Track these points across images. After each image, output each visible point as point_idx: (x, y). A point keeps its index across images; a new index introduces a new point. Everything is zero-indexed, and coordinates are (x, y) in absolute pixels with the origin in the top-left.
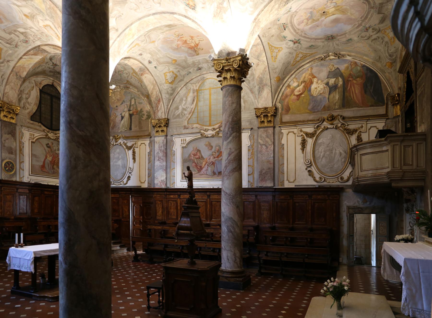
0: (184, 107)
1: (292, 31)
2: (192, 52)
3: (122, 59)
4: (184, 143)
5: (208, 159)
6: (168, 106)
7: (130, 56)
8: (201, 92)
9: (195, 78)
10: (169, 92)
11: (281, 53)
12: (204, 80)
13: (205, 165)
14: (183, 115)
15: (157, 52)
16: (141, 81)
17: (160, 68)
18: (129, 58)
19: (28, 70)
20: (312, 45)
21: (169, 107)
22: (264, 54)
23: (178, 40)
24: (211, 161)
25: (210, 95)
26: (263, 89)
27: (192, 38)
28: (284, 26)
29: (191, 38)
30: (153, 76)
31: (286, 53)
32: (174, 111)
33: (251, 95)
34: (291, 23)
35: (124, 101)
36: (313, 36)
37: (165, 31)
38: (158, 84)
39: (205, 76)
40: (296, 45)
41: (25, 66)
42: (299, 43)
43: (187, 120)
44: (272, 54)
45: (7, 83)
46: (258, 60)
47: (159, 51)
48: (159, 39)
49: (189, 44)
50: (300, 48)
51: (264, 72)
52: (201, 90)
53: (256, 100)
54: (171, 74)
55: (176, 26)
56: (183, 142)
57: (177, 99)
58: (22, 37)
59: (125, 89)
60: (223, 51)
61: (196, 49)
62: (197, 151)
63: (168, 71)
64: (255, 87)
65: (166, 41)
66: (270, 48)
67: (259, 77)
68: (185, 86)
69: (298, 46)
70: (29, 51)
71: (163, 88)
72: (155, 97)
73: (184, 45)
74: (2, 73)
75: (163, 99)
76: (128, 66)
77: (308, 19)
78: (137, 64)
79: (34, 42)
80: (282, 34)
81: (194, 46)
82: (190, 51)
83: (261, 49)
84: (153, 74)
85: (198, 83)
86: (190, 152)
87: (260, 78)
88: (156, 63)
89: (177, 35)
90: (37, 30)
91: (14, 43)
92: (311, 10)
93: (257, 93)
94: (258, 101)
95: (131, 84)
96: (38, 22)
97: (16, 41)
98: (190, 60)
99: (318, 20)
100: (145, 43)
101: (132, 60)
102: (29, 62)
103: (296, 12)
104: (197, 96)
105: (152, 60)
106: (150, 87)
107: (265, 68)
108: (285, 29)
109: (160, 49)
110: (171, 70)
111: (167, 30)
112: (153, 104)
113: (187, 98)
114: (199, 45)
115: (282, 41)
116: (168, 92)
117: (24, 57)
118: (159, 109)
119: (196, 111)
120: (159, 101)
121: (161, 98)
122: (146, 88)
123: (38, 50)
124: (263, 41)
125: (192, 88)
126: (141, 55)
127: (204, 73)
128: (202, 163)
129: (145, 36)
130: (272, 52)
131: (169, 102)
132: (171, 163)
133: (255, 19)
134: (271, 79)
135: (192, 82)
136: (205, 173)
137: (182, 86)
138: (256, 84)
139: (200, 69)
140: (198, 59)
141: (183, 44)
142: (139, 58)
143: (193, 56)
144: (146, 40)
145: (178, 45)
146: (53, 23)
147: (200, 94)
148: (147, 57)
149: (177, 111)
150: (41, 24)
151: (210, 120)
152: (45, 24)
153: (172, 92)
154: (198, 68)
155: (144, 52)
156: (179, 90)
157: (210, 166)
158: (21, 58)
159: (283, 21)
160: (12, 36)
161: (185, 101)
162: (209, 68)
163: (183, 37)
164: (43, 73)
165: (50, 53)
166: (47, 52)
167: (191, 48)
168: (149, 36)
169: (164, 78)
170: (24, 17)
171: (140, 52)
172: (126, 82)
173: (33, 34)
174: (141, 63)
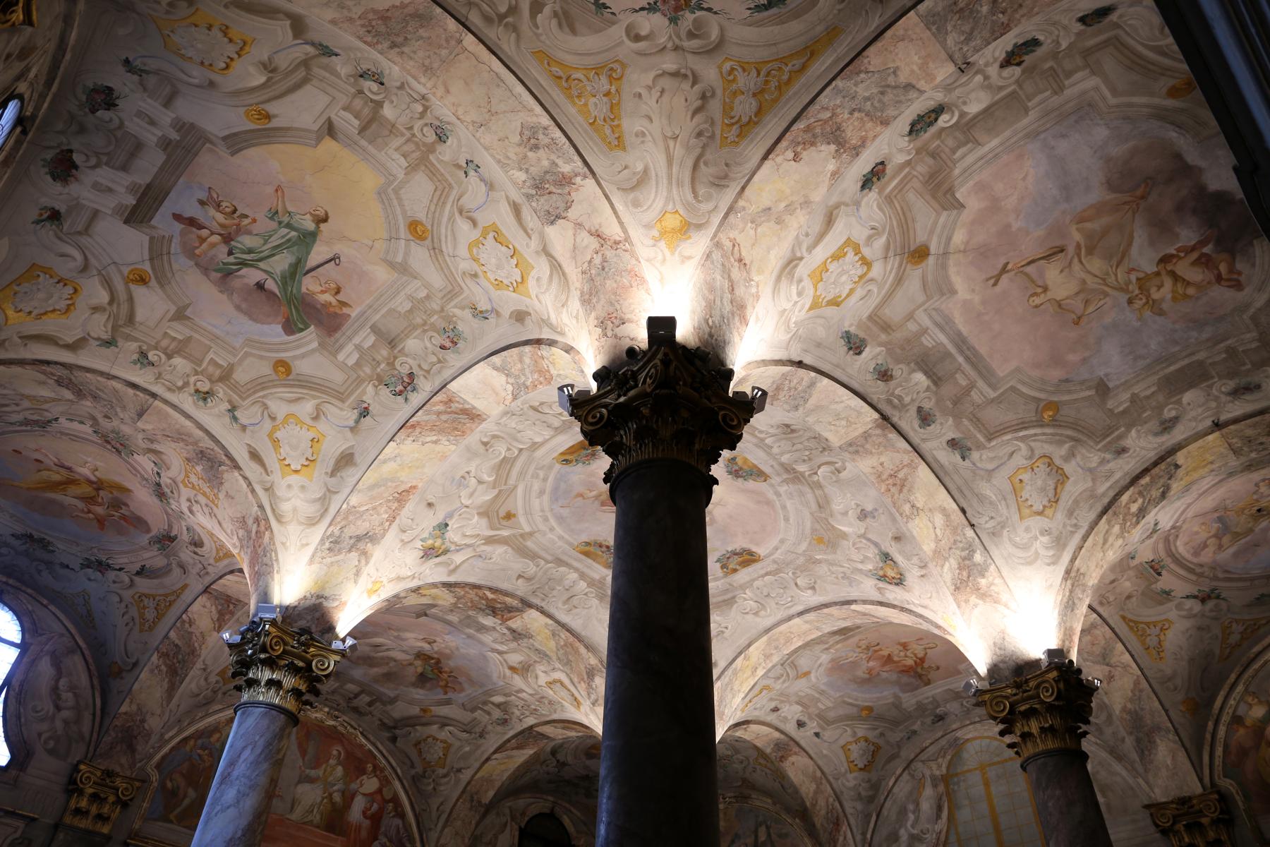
1: (1182, 572)
2: (913, 680)
3: (729, 729)
6: (864, 834)
7: (749, 719)
8: (956, 780)
9: (932, 744)
10: (864, 793)
11: (1170, 634)
12: (957, 747)
15: (817, 695)
16: (781, 776)
17: (828, 734)
18: (747, 722)
19: (498, 784)
20: (1263, 595)
21: (869, 836)
22: (1120, 646)
23: (869, 659)
25: (987, 784)
26: (1152, 742)
27: (905, 646)
28: (1152, 567)
29: (901, 648)
30: (811, 758)
31: (1187, 630)
33: (1118, 767)
34: (1170, 554)
35: (737, 836)
36: (1256, 572)
37: (833, 645)
38: (831, 778)
39: (959, 734)
40: (1210, 604)
41: (494, 777)
42: (1218, 597)
44: (1143, 643)
45: (447, 820)
46: (1108, 665)
47: (822, 692)
48: (820, 666)
49: (899, 662)
50: (1229, 610)
51: (1137, 693)
52: (957, 775)
53: (1140, 781)
54: (863, 744)
55: (858, 627)
57: (890, 810)
58: (497, 714)
59: (737, 802)
60: (1001, 665)
61: (919, 670)
63: (850, 739)
64: (1123, 740)
65: (837, 667)
66: (1131, 628)
67: (1124, 709)
68: (906, 772)
69: (1216, 605)
70: (509, 740)
71: (843, 785)
72: (823, 812)
73: (887, 668)
74: (441, 800)
75: (849, 816)
76: (745, 741)
77: (1217, 536)
78: (767, 735)
79: (521, 720)
80: (1153, 586)
81: (913, 663)
82: (905, 679)
83: (1107, 637)
84: (811, 752)
85: (944, 757)
87: (1129, 712)
88: (818, 724)
89: (864, 647)
90: (531, 695)
91: (478, 730)
92: (1216, 515)
93: (1134, 756)
94: (1147, 783)
95: (753, 787)
96: (537, 677)
97: (483, 724)
98: (909, 701)
99: (1251, 530)
100: (784, 682)
101: (753, 727)
102: (503, 767)
103: (1173, 527)
104: (948, 794)
105: (805, 719)
106: (807, 789)
107: (1137, 683)
108: (1159, 574)
109: (823, 687)
110: (860, 733)
111: (837, 643)
112: (821, 832)
113: (918, 805)
114: (927, 661)
115: (1161, 604)
116: (859, 794)
117: (496, 756)
119: (952, 838)
120: (837, 824)
121: (841, 815)
122: (796, 791)
123: (529, 735)
124: (1105, 614)
125: (928, 773)
126: (776, 710)
127: (954, 726)
129: (782, 665)
130: (1142, 636)
131: (869, 822)
133: (1068, 572)
134: (1166, 711)
135: (924, 756)
137: (898, 772)
138: (1123, 733)
139: (941, 718)
140: (930, 694)
141: (883, 665)
142: (771, 718)
143: (916, 689)
144: (788, 674)
145: (870, 671)
146: (567, 675)
147: (956, 787)
148: (792, 712)
150: (543, 679)
152: (550, 679)
153: (870, 793)
154: (936, 716)
155: (782, 702)
156: (891, 784)
158: (488, 759)
159: (1146, 555)
160: (478, 714)
161: (914, 812)
162: (968, 711)
163: (881, 650)
164: (534, 787)
165: (553, 739)
166: (548, 738)
167: (906, 671)
168: (792, 662)
169: (843, 759)
170: (508, 672)
171: (773, 705)
172: (739, 784)
173: (521, 703)
174: (777, 729)
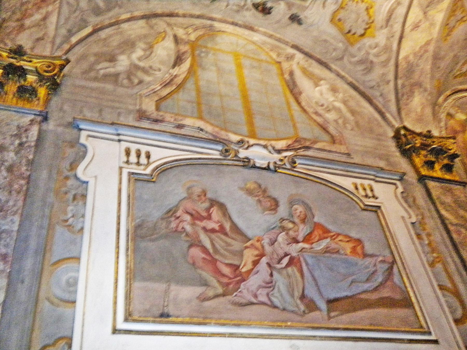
0: (142, 64)
4: (138, 164)
5: (266, 242)
13: (256, 263)
14: (136, 81)
21: (74, 40)
24: (281, 253)
32: (92, 59)
43: (156, 98)
56: (133, 158)
62: (206, 205)
86: (172, 201)
118: (27, 22)
119: (190, 85)
128: (240, 254)
132: (51, 227)
136: (263, 298)
137: (137, 14)
149: (106, 64)
151: (251, 123)
157: (280, 271)
